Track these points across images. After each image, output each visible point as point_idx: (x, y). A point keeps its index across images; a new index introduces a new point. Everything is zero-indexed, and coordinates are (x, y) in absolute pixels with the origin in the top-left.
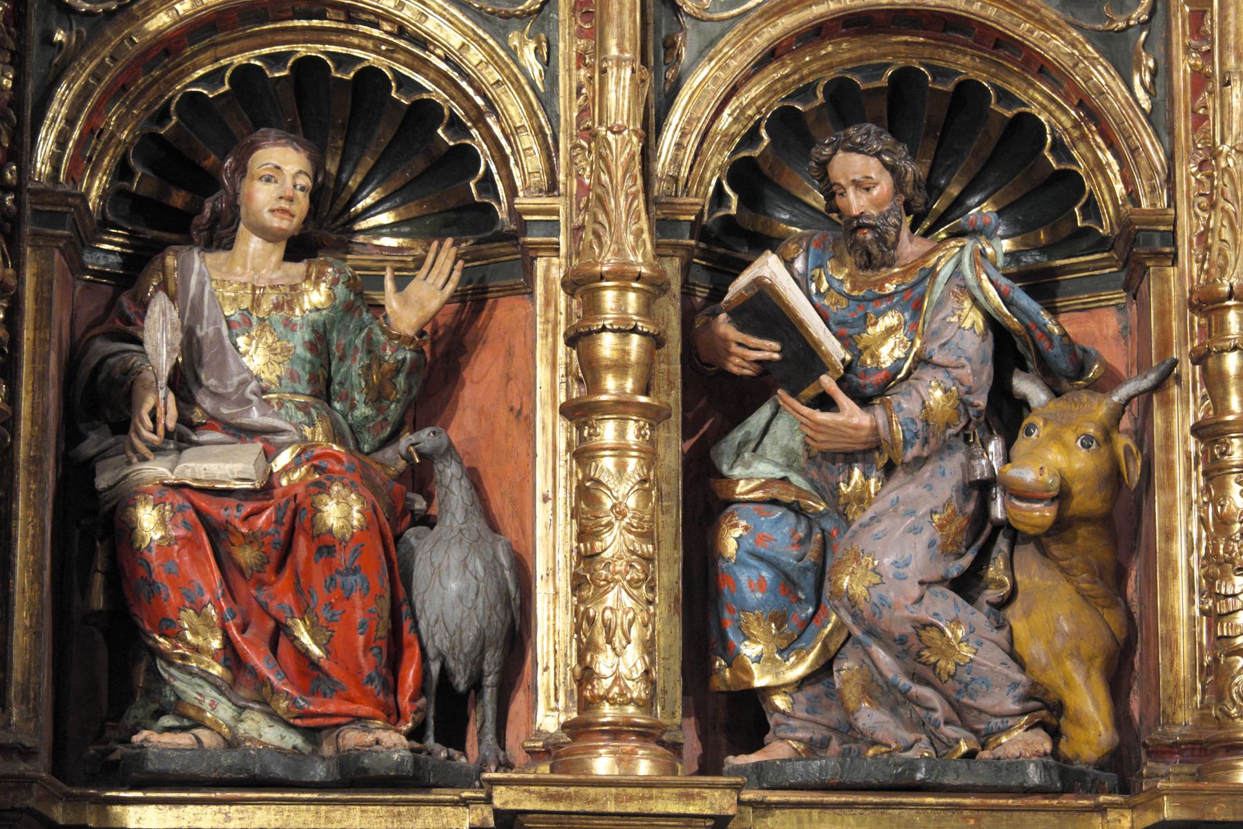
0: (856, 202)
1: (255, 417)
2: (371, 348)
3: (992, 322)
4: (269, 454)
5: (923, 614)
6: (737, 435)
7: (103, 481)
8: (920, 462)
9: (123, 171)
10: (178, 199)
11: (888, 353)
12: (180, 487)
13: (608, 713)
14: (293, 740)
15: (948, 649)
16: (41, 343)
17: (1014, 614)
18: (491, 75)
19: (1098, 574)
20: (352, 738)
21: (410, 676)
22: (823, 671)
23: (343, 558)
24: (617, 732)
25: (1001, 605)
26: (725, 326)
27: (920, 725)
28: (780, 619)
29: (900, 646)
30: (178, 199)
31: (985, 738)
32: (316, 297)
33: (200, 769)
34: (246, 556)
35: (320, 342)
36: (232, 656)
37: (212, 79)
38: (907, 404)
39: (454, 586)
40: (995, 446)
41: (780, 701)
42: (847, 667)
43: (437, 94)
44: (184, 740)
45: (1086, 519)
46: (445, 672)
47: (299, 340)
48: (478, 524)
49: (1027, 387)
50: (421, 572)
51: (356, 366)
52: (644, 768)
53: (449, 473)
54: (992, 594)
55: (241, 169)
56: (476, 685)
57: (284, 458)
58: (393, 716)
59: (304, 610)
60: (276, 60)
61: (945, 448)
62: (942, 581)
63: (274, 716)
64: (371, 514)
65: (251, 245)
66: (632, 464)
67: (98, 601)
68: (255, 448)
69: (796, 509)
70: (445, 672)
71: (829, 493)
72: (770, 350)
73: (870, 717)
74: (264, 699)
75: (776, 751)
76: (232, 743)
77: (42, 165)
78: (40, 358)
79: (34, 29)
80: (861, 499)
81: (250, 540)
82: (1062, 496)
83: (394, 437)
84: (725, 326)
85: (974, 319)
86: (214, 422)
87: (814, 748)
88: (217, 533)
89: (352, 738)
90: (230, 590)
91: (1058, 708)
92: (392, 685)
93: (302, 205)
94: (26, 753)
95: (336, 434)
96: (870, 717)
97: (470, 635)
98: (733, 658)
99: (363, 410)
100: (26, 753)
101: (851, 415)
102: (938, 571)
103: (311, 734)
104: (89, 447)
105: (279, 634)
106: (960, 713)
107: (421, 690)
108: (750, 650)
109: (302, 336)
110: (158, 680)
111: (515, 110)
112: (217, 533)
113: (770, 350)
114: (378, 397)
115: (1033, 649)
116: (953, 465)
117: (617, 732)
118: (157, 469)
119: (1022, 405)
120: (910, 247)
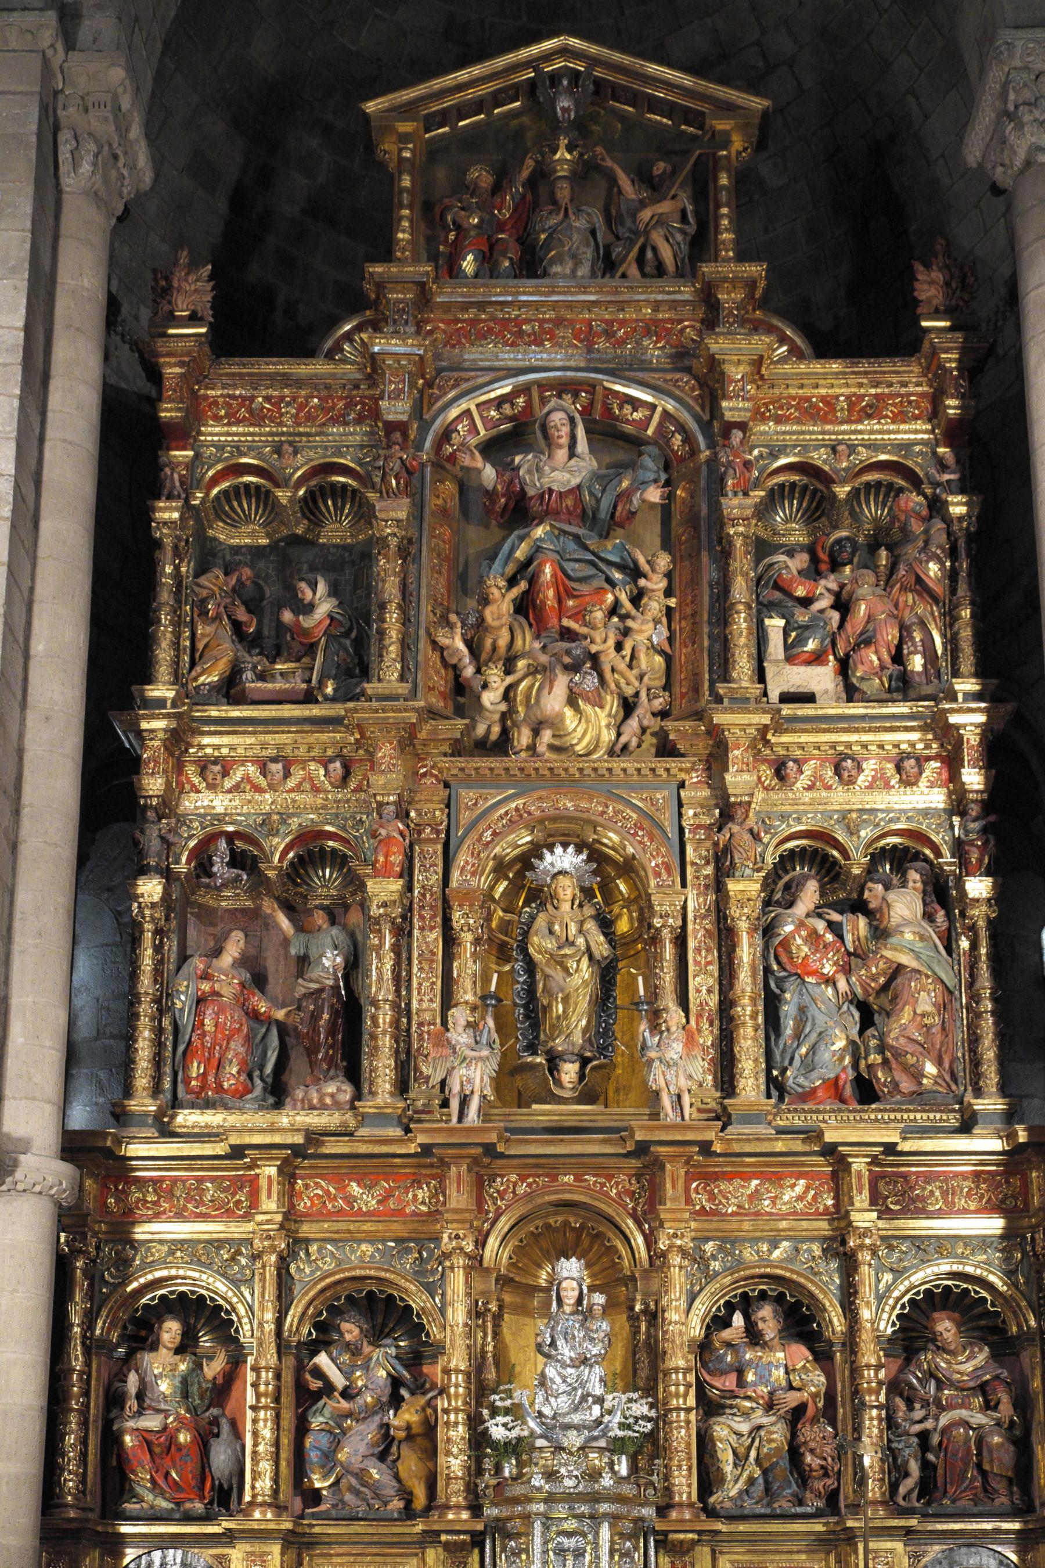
0: (348, 1337)
1: (163, 1406)
2: (199, 1383)
3: (389, 1374)
4: (166, 1418)
5: (362, 1466)
6: (314, 1408)
7: (115, 1428)
8: (365, 1419)
9: (125, 1328)
10: (143, 1333)
11: (360, 1383)
12: (137, 1429)
13: (260, 1499)
14: (171, 1506)
15: (371, 1477)
16: (98, 1385)
17: (399, 1464)
18: (235, 1300)
19: (425, 1451)
20: (188, 1505)
21: (208, 1484)
22: (337, 1482)
23: (184, 1452)
24: (263, 1504)
25: (395, 1461)
26: (308, 1376)
27: (364, 1500)
28: (323, 1467)
29: (356, 1475)
30: (143, 1333)
31: (386, 1504)
32: (183, 1367)
33: (142, 1515)
34: (157, 1450)
35: (185, 1381)
36: (153, 1481)
37: (153, 1299)
38: (359, 1400)
39: (222, 1457)
40: (391, 1412)
41: (325, 1493)
42: (344, 1481)
43: (221, 1302)
44: (138, 1506)
45: (418, 1435)
46: (221, 1484)
47: (177, 1381)
48: (232, 1437)
49: (404, 1392)
50: (213, 1453)
51: (196, 1387)
52: (687, 1517)
53: (223, 1421)
54: (392, 1458)
55: (160, 1327)
56: (231, 1488)
57: (171, 1419)
58: (202, 1498)
59: (174, 1467)
60: (172, 1292)
61: (375, 1413)
62: (372, 1455)
63: (165, 1499)
64: (194, 1438)
65: (163, 1351)
66: (269, 1424)
67: (114, 1463)
68: (161, 1416)
69: (330, 1432)
70: (221, 1484)
71: (340, 1427)
72: (319, 1384)
73: (348, 1497)
74: (162, 1494)
75: (323, 1507)
76: (152, 1507)
77: (98, 1332)
78: (97, 1390)
79: (97, 1289)
80: (350, 1428)
81: (159, 1445)
82: (408, 1427)
83: (207, 1409)
84: (308, 1376)
85: (384, 1374)
86: (150, 1408)
87: (334, 1506)
88: (149, 1444)
89: (188, 1505)
90: (153, 1460)
91: (411, 1493)
92: (202, 1488)
93: (179, 1338)
94: (92, 1510)
95: (188, 1411)
96: (348, 1497)
97: (227, 1473)
98: (310, 1480)
99: (198, 1402)
100: (92, 1510)
101: (344, 1404)
102: (370, 1452)
103: (178, 1504)
104: (112, 1415)
105: (167, 1475)
106: (377, 1496)
107: (212, 1489)
108: (315, 1477)
109: (178, 1379)
110: (132, 1489)
111: (241, 1310)
112: (149, 1444)
113: (319, 1384)
114: (202, 1398)
115: (403, 1474)
116: (377, 1419)
117: (263, 1504)
118: (131, 1424)
119: (402, 1399)
120: (367, 1349)
